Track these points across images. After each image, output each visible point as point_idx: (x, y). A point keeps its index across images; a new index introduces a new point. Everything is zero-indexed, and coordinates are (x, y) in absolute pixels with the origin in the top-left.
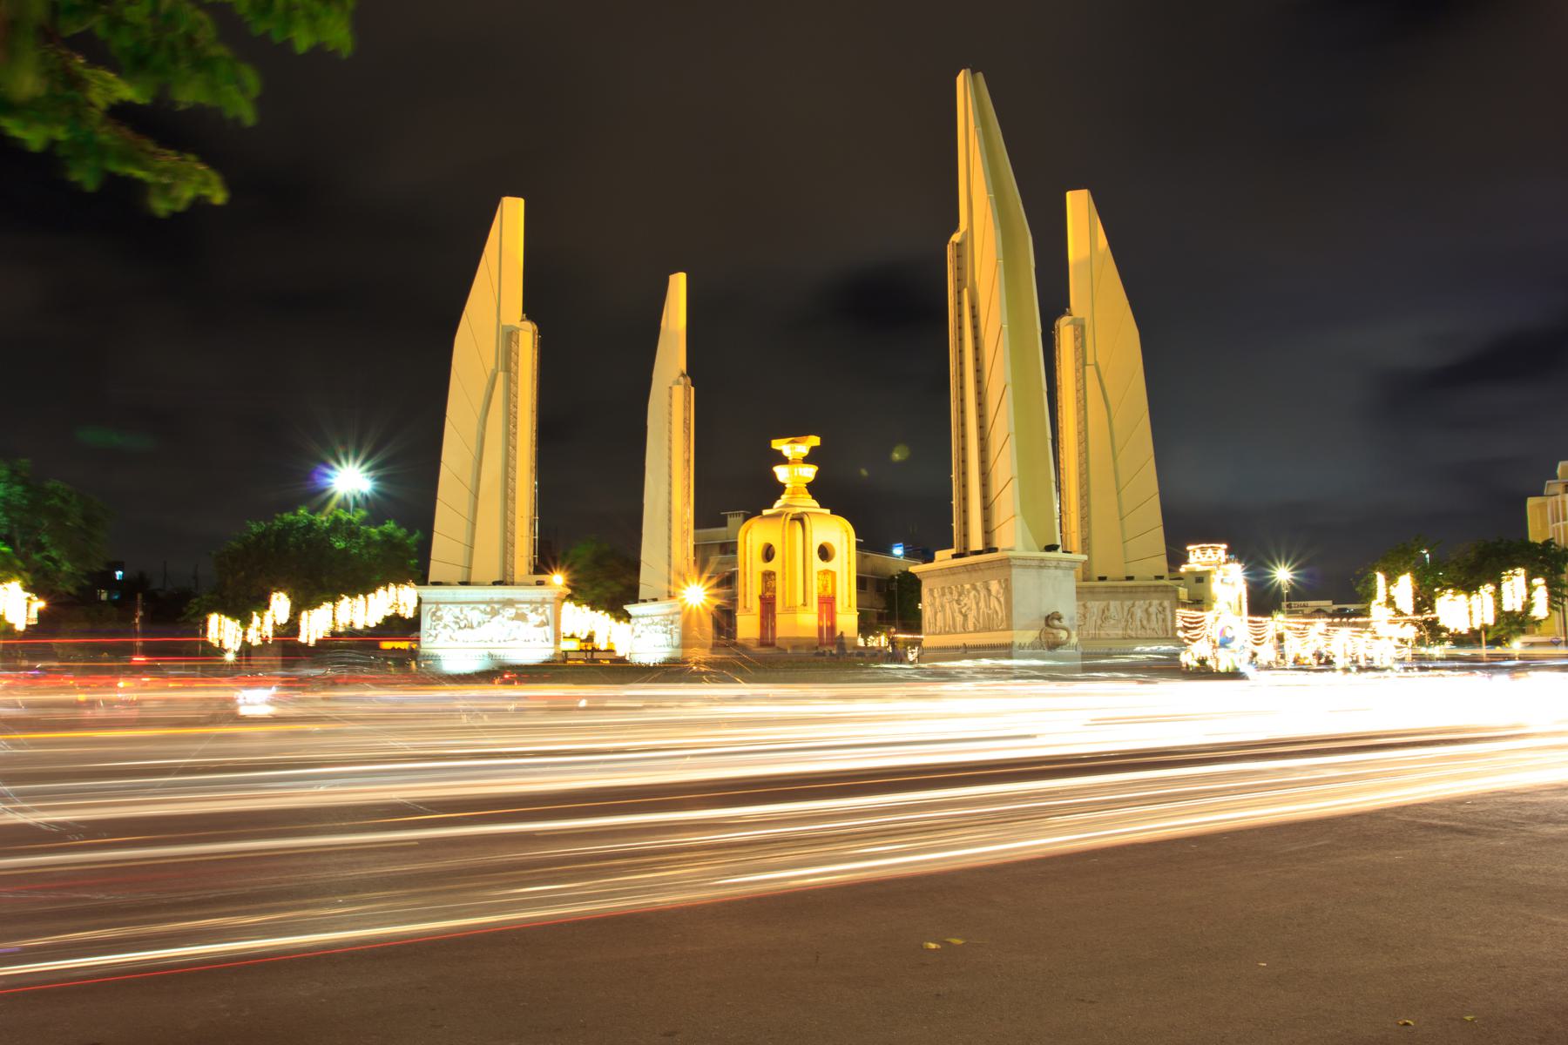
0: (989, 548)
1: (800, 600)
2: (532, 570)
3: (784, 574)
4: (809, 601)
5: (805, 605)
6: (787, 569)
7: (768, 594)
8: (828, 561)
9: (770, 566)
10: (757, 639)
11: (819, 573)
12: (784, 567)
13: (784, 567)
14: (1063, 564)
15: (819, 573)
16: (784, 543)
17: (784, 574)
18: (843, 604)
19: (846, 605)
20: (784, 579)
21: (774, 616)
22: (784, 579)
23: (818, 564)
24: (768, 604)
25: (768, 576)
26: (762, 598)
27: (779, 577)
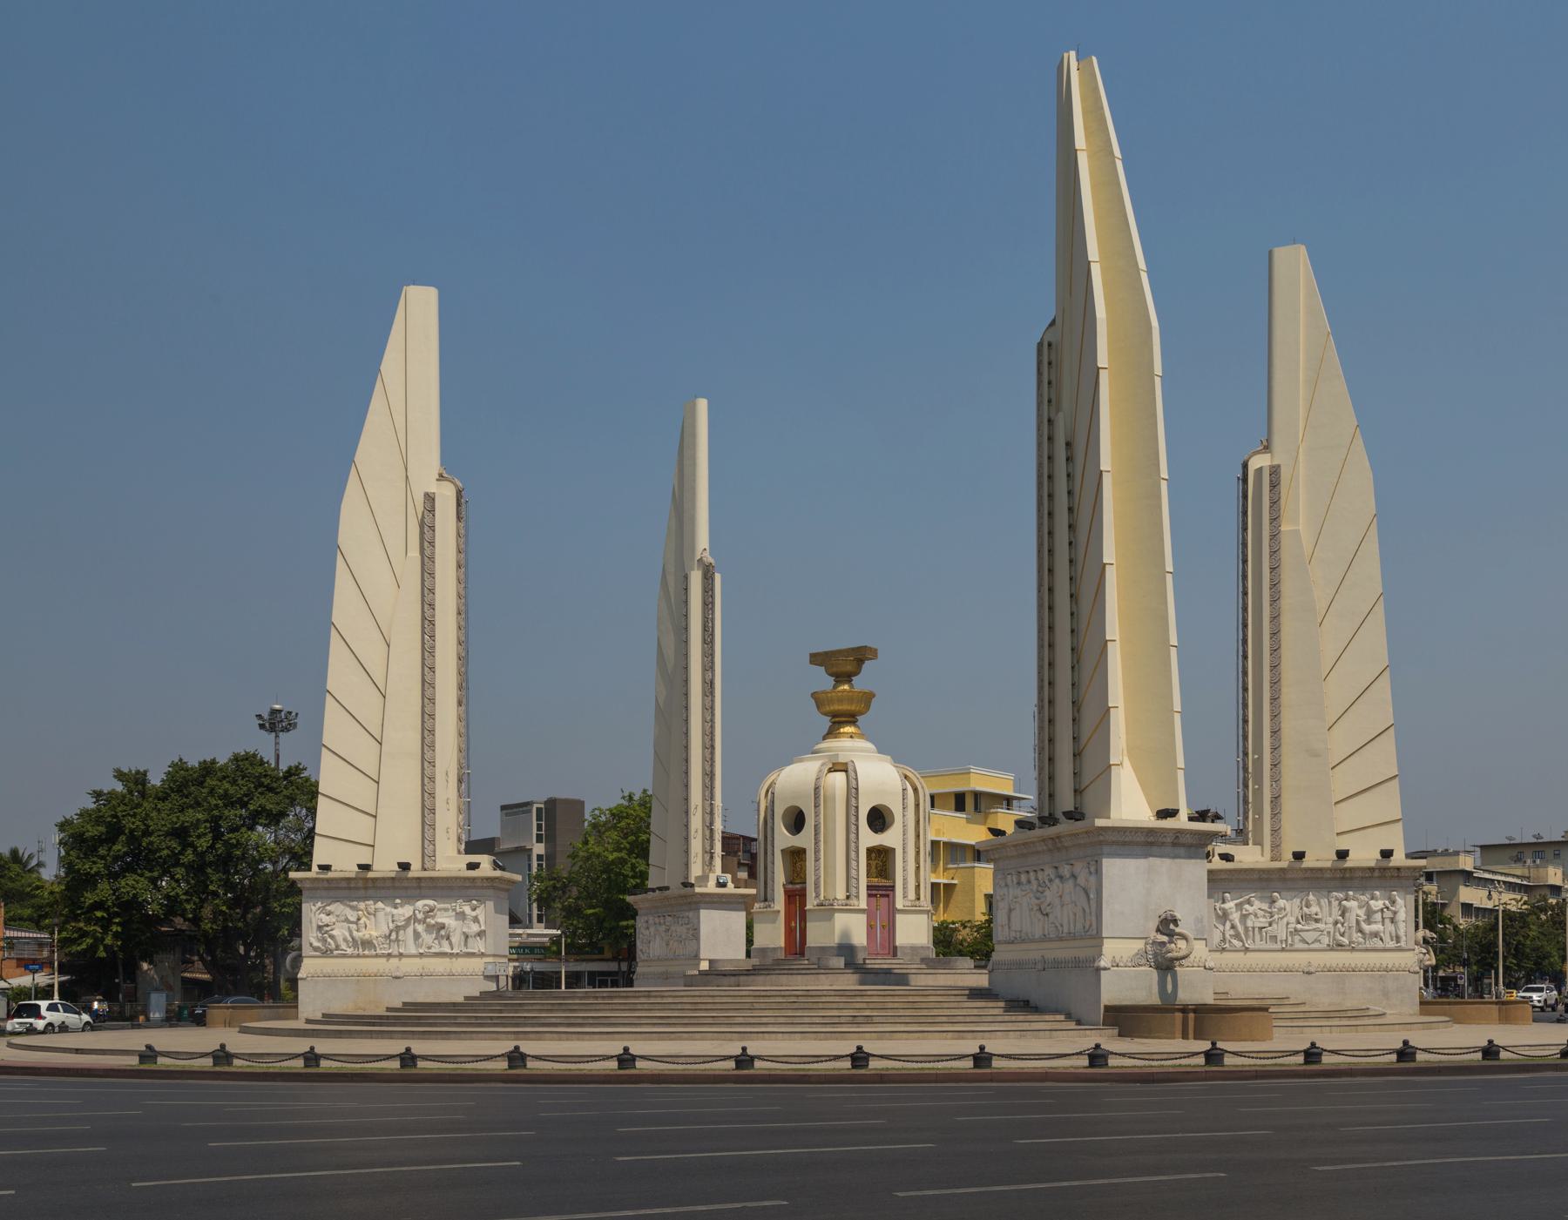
0: (1075, 815)
1: (840, 894)
2: (463, 846)
3: (817, 851)
4: (853, 891)
6: (822, 843)
8: (876, 832)
11: (870, 851)
14: (1188, 839)
15: (870, 851)
16: (817, 806)
17: (817, 851)
18: (905, 897)
20: (817, 860)
21: (803, 919)
22: (817, 860)
23: (868, 839)
27: (810, 856)
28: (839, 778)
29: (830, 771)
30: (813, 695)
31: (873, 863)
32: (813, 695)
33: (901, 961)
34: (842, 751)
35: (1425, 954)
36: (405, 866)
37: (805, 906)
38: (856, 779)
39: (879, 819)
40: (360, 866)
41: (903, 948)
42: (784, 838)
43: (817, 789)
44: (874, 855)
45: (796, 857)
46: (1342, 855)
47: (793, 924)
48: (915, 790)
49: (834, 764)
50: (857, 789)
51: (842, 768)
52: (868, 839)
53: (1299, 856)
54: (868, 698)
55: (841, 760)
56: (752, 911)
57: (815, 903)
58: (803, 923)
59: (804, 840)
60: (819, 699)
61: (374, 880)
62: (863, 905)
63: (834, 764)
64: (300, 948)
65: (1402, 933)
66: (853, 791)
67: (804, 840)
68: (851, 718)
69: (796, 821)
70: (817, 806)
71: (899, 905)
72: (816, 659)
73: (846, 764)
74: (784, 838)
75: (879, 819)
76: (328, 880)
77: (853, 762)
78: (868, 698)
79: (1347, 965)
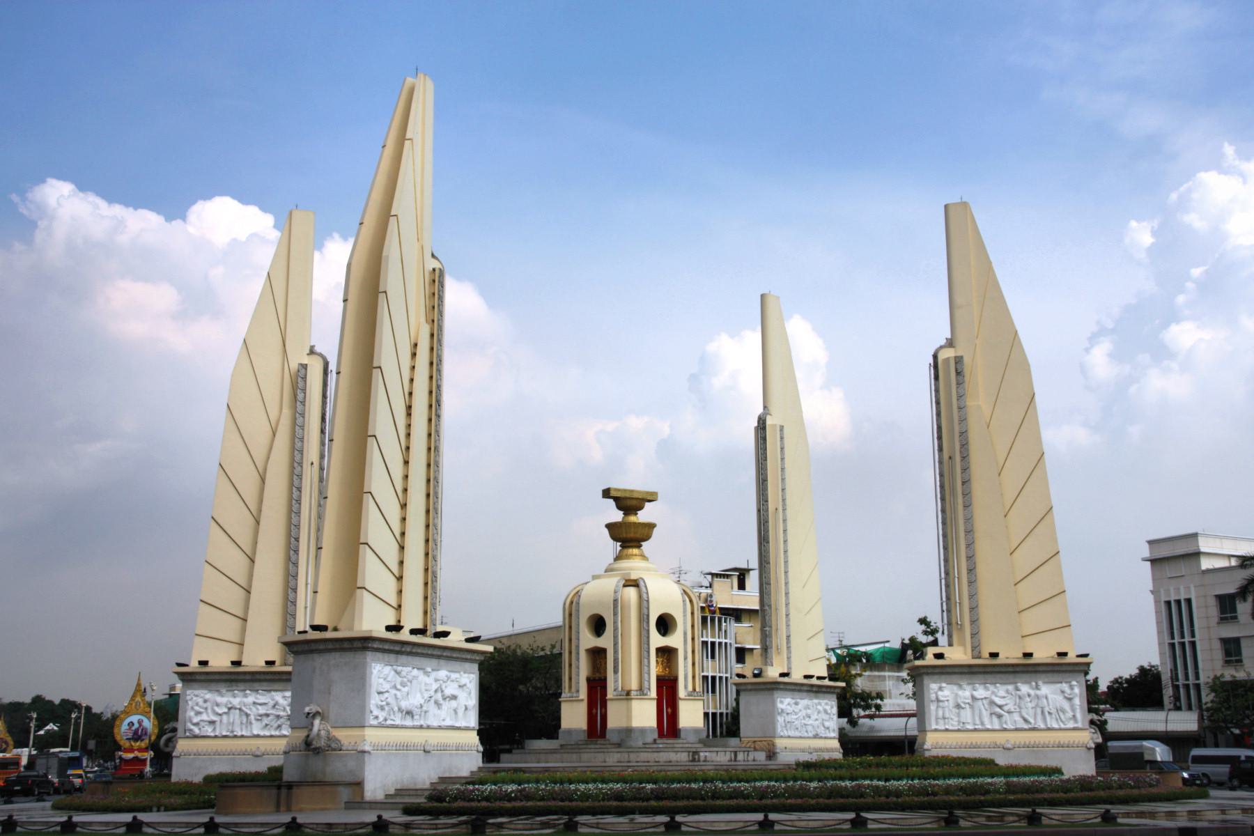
1: (634, 685)
3: (616, 652)
5: (641, 689)
7: (597, 675)
9: (601, 642)
10: (585, 731)
12: (616, 644)
13: (616, 644)
16: (615, 614)
17: (616, 652)
18: (686, 687)
19: (690, 688)
23: (657, 640)
24: (597, 687)
25: (598, 655)
26: (588, 680)
28: (631, 593)
29: (625, 586)
30: (609, 526)
31: (660, 660)
32: (609, 526)
33: (685, 741)
34: (632, 570)
35: (1094, 733)
36: (270, 663)
37: (606, 696)
38: (647, 593)
39: (665, 624)
40: (233, 663)
41: (686, 730)
42: (588, 640)
43: (615, 601)
45: (598, 655)
46: (1028, 655)
47: (594, 711)
48: (691, 601)
49: (626, 580)
50: (648, 601)
51: (635, 584)
52: (657, 640)
53: (994, 655)
54: (651, 526)
55: (633, 577)
56: (560, 700)
57: (615, 693)
58: (603, 710)
59: (605, 641)
60: (614, 530)
61: (245, 673)
62: (653, 693)
63: (626, 580)
64: (175, 730)
65: (1079, 716)
66: (643, 603)
67: (605, 641)
69: (598, 625)
70: (615, 614)
71: (682, 693)
72: (606, 493)
73: (635, 581)
74: (588, 640)
75: (665, 624)
76: (207, 673)
77: (643, 579)
78: (651, 526)
79: (1037, 743)
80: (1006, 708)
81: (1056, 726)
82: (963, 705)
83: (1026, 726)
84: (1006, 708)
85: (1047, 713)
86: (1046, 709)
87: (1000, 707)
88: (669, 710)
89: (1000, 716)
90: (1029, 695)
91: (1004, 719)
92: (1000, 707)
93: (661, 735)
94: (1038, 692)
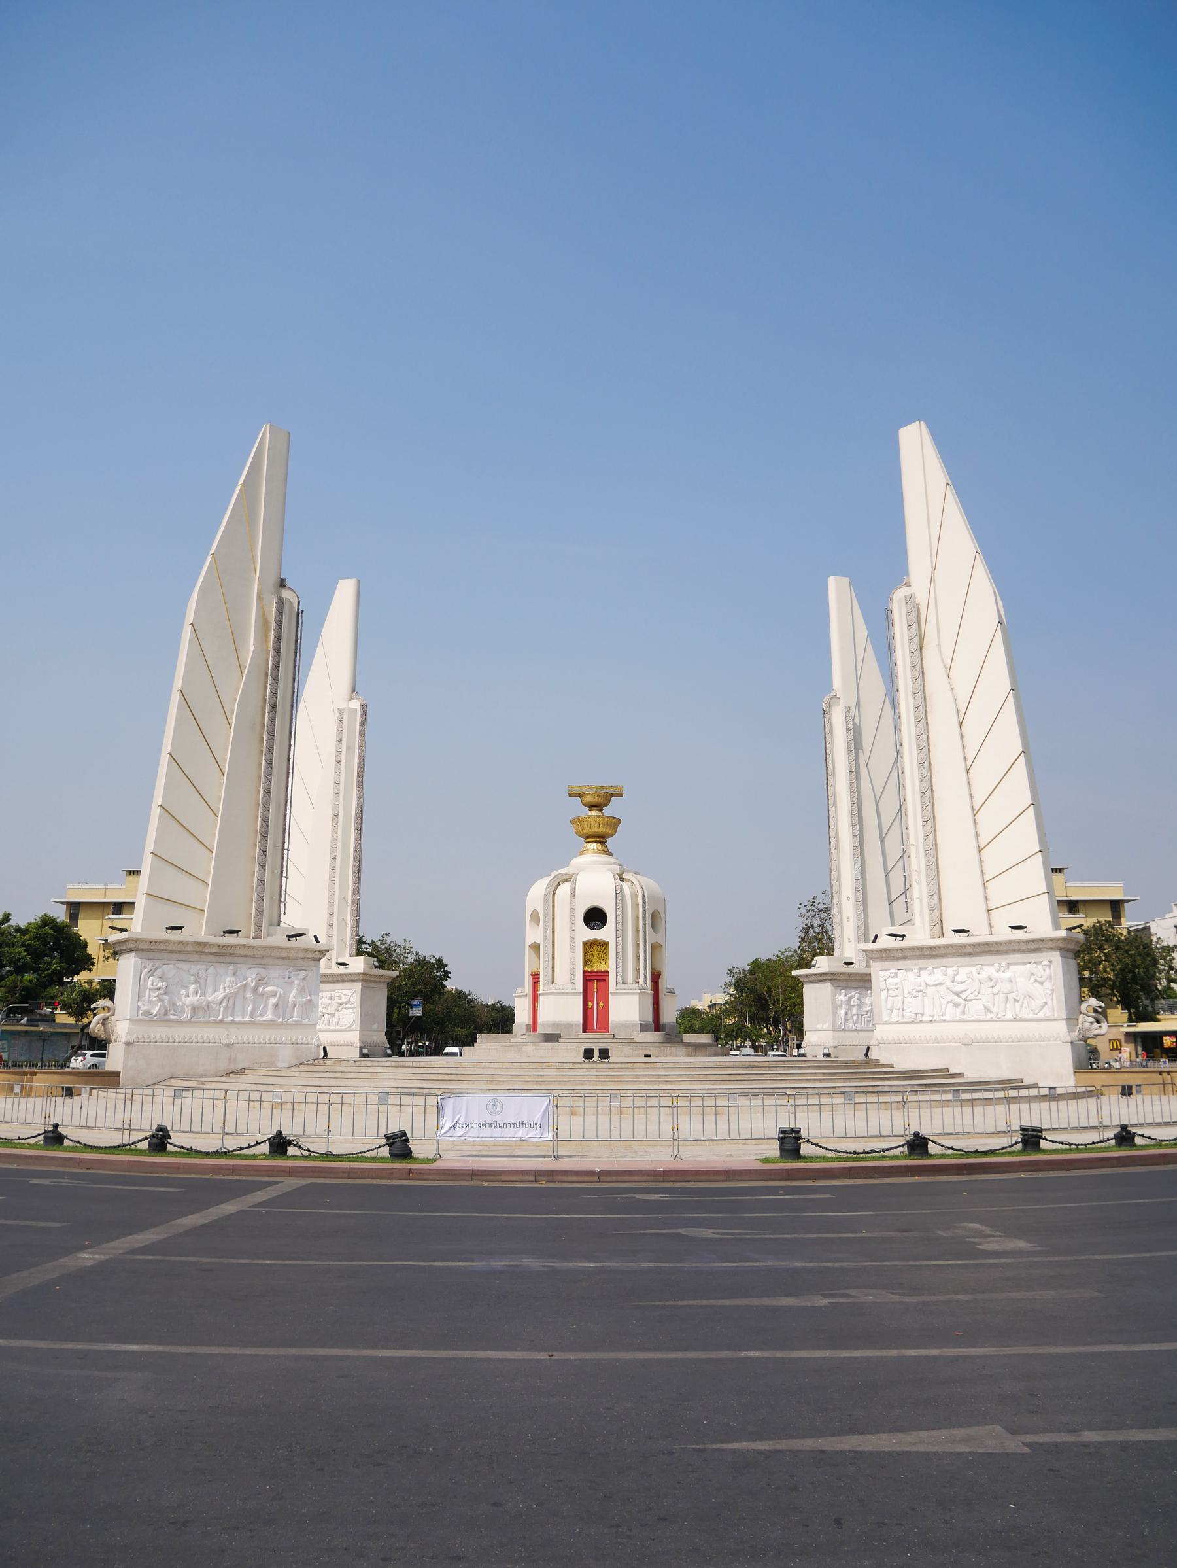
11: (585, 944)
15: (585, 944)
44: (596, 947)
68: (601, 839)
71: (612, 986)
75: (595, 917)
80: (964, 995)
81: (1025, 1016)
82: (915, 993)
83: (989, 1016)
84: (964, 995)
85: (1011, 1000)
86: (1011, 996)
87: (957, 994)
88: (601, 1004)
89: (957, 1005)
90: (991, 980)
91: (961, 1007)
92: (957, 994)
93: (584, 1031)
94: (1001, 975)
